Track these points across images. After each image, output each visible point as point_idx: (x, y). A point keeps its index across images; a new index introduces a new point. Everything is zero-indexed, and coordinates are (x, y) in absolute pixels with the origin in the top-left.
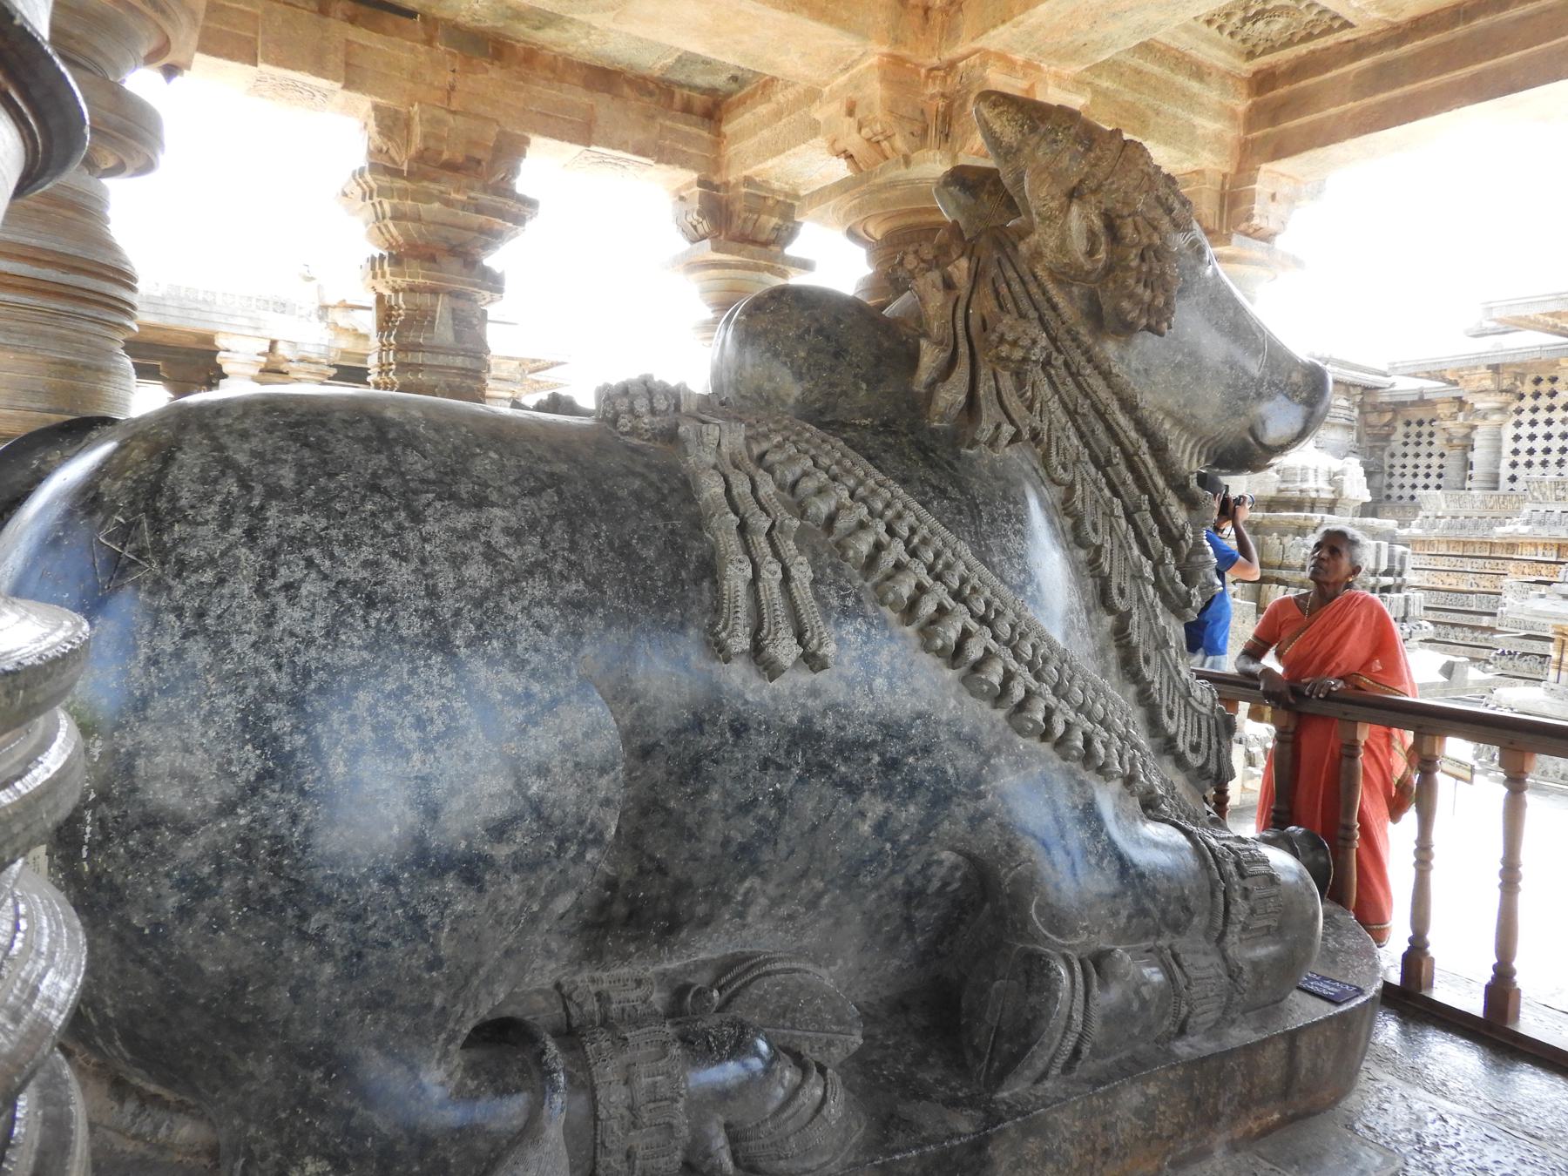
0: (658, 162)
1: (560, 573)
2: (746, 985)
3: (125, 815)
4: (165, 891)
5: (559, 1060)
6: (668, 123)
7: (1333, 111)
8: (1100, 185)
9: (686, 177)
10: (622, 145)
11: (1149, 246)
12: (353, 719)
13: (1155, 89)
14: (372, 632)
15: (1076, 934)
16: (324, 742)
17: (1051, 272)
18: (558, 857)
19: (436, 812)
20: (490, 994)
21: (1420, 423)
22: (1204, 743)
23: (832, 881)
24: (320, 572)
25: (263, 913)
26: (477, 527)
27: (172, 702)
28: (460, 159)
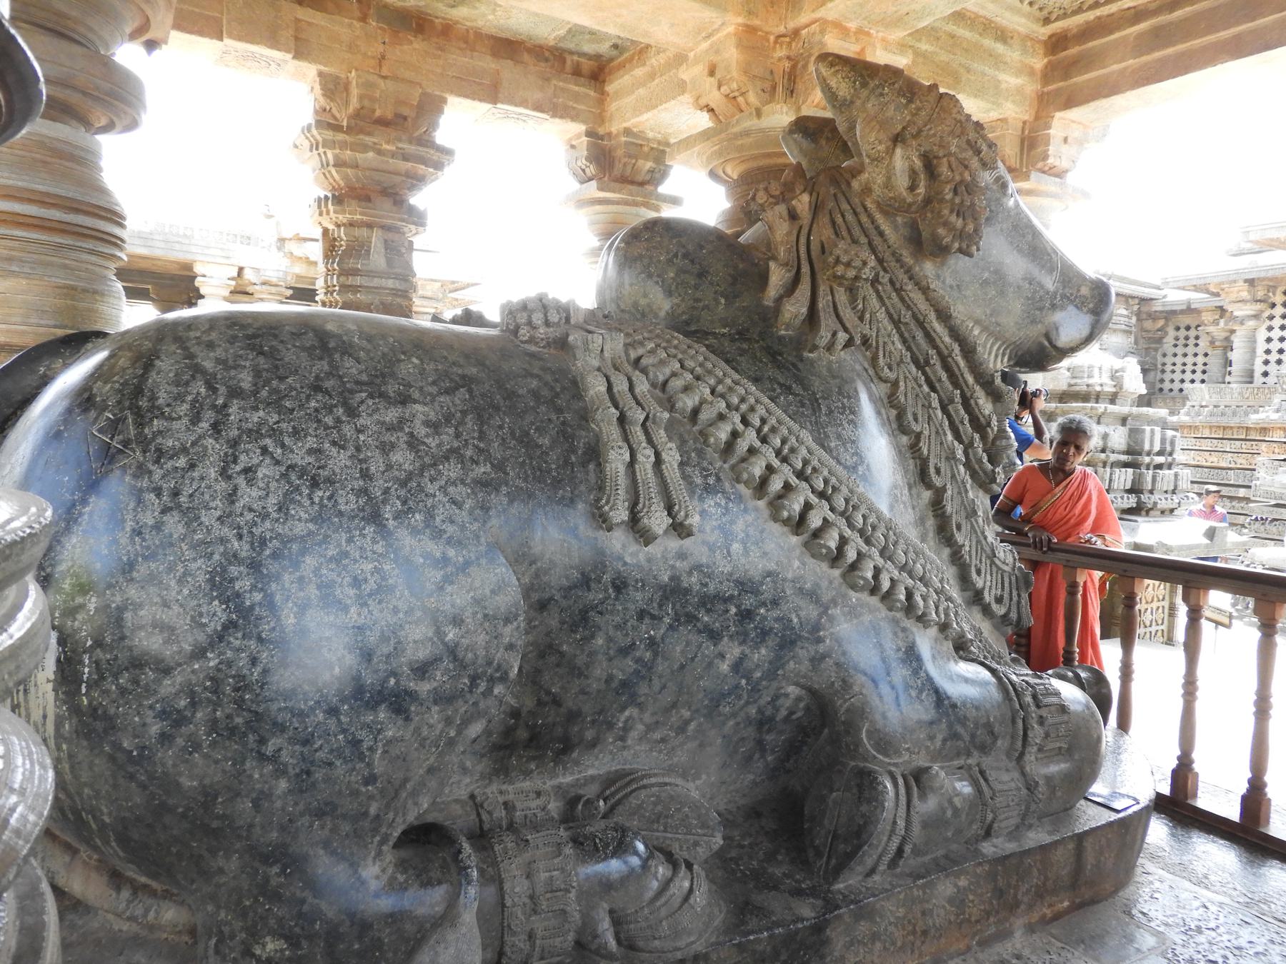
0: (554, 116)
1: (471, 458)
2: (626, 796)
3: (116, 658)
4: (149, 720)
7: (1116, 67)
8: (920, 131)
9: (576, 129)
10: (523, 103)
11: (962, 181)
12: (301, 579)
13: (966, 50)
14: (316, 508)
15: (900, 756)
16: (278, 598)
17: (878, 205)
18: (471, 692)
19: (370, 655)
20: (416, 804)
21: (1188, 328)
22: (1006, 596)
23: (697, 711)
25: (229, 739)
26: (402, 421)
27: (153, 566)
28: (389, 115)
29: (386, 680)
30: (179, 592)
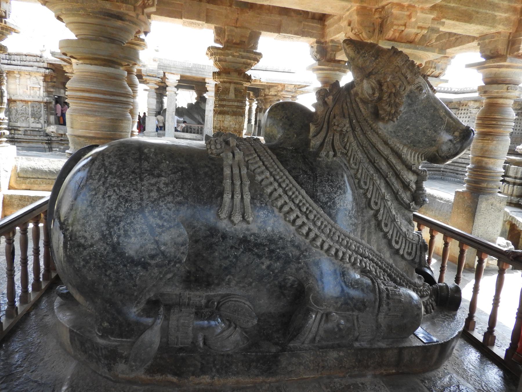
0: (303, 36)
1: (177, 195)
2: (225, 302)
3: (74, 244)
4: (81, 261)
5: (162, 312)
6: (306, 23)
8: (379, 71)
9: (313, 40)
11: (391, 93)
13: (476, 4)
14: (126, 208)
15: (322, 307)
16: (113, 233)
22: (414, 253)
24: (116, 193)
26: (157, 183)
28: (238, 42)
29: (141, 259)
30: (89, 229)
